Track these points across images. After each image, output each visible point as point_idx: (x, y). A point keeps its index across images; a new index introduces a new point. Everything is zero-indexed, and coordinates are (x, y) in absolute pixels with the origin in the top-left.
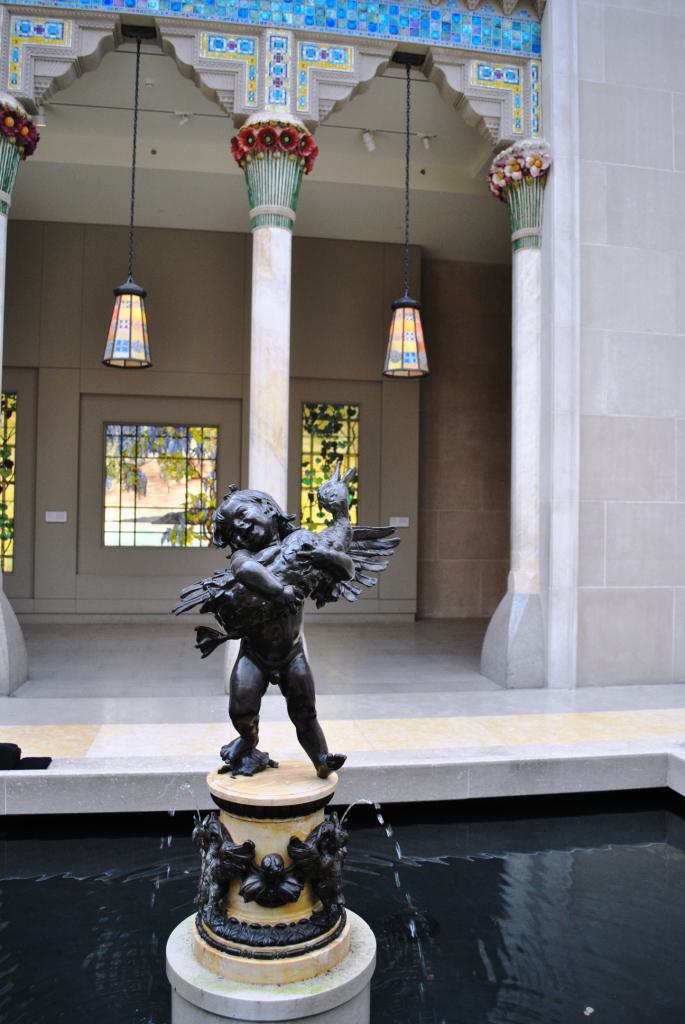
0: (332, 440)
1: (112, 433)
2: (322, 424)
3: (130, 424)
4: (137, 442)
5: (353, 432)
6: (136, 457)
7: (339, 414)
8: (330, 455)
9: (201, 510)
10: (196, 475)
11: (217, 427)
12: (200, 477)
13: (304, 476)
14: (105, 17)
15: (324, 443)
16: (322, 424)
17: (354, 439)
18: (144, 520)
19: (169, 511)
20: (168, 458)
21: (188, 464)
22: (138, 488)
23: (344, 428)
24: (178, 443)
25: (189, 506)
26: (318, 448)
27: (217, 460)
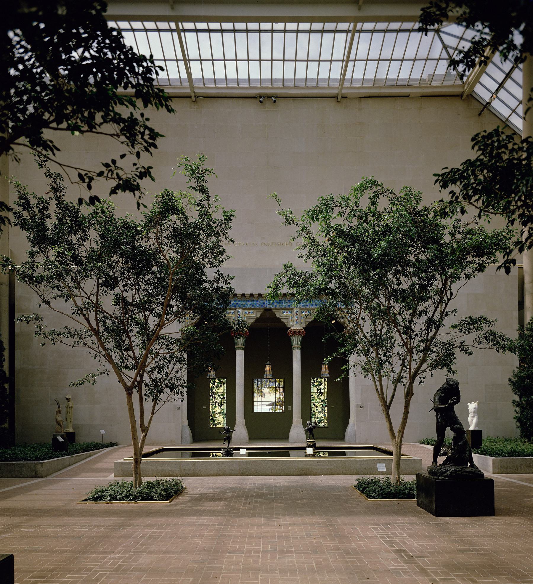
2: (317, 384)
8: (319, 392)
14: (262, 309)
15: (317, 389)
16: (317, 384)
23: (323, 385)
26: (316, 390)
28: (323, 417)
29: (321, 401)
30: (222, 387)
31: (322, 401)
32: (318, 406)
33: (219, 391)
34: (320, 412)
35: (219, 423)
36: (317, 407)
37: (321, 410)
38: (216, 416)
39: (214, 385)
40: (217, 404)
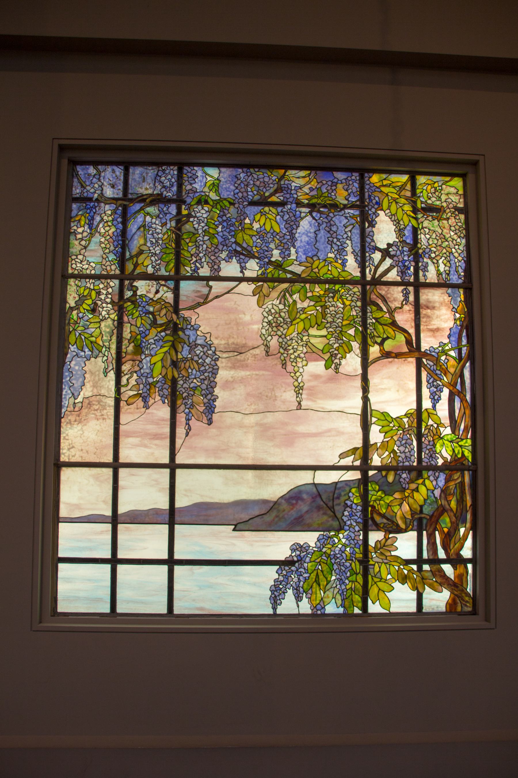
20: (296, 279)
24: (330, 224)
25: (376, 461)
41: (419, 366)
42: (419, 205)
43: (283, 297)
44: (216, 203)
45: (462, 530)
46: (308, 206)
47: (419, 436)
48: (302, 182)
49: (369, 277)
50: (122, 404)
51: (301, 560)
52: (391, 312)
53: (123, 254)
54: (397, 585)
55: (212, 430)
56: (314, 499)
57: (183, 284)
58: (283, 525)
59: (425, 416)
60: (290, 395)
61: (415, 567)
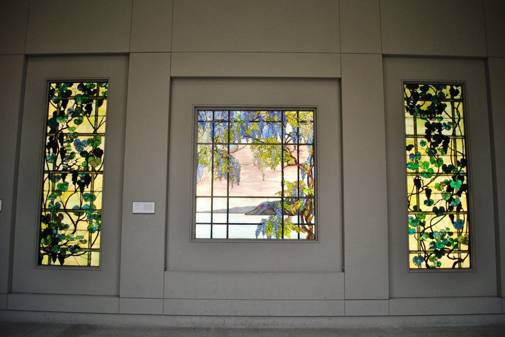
0: (436, 121)
1: (204, 119)
2: (425, 105)
3: (222, 109)
4: (229, 127)
5: (457, 111)
6: (229, 144)
7: (441, 94)
8: (435, 137)
9: (298, 198)
10: (292, 161)
11: (313, 109)
12: (297, 163)
13: (409, 160)
16: (425, 105)
17: (459, 121)
18: (237, 211)
19: (265, 200)
20: (263, 143)
21: (283, 150)
22: (231, 175)
23: (448, 109)
25: (286, 195)
26: (422, 130)
27: (314, 144)
28: (453, 229)
29: (444, 167)
30: (93, 113)
31: (447, 170)
32: (434, 190)
33: (80, 129)
34: (439, 212)
35: (75, 249)
36: (428, 192)
37: (443, 204)
38: (66, 220)
39: (65, 105)
40: (69, 178)
41: (299, 168)
42: (299, 121)
43: (259, 149)
44: (240, 122)
45: (311, 215)
46: (266, 122)
47: (298, 188)
48: (264, 115)
49: (284, 143)
50: (214, 180)
51: (264, 223)
52: (290, 153)
53: (213, 137)
54: (292, 231)
55: (239, 187)
56: (268, 206)
57: (230, 146)
58: (259, 213)
59: (300, 182)
60: (261, 177)
61: (297, 226)
